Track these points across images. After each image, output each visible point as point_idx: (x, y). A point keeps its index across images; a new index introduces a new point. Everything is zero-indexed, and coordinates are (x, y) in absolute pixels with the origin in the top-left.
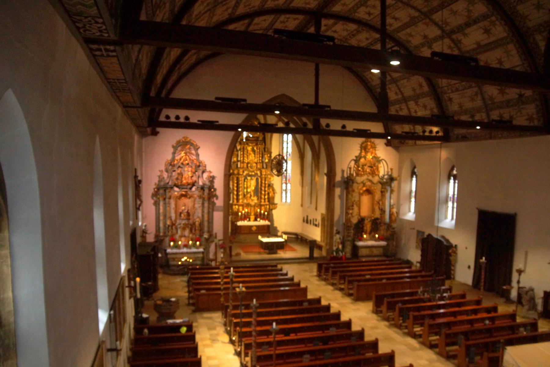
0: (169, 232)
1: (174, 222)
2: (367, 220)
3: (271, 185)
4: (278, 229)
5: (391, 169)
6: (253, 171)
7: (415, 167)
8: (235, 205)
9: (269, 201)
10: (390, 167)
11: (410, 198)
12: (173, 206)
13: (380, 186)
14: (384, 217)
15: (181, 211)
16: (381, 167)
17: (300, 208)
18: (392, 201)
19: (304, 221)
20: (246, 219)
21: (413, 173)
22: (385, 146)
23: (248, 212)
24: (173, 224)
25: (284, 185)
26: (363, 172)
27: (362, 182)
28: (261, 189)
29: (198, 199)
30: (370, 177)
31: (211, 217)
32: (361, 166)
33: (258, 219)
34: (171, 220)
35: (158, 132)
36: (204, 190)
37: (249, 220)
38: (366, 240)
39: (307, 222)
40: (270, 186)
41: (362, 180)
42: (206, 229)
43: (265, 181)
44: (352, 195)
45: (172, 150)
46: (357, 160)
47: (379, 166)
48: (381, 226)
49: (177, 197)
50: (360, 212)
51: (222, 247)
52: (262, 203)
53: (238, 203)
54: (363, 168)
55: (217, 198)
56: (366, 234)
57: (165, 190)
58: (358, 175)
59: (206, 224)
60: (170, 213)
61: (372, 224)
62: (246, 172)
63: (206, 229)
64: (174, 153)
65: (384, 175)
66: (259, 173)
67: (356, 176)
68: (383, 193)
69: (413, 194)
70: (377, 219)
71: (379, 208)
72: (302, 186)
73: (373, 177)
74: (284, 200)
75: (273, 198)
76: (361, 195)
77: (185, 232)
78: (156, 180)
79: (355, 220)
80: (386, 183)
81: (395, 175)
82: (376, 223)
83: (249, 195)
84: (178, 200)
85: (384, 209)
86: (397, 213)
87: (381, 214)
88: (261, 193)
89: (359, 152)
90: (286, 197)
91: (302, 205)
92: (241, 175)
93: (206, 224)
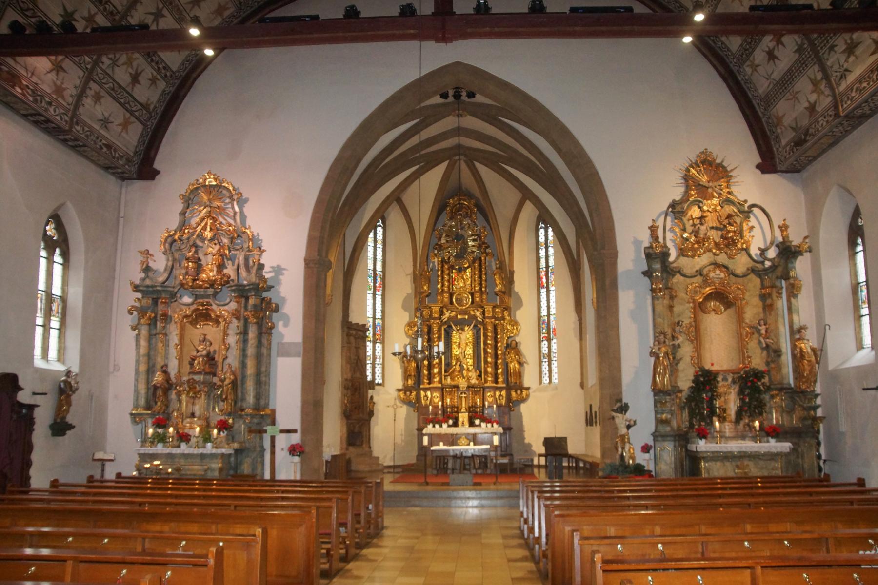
0: (156, 403)
1: (173, 380)
2: (725, 379)
3: (514, 342)
4: (534, 448)
5: (783, 228)
6: (465, 312)
7: (857, 213)
8: (426, 390)
9: (507, 381)
10: (777, 222)
11: (857, 308)
12: (174, 339)
13: (755, 281)
14: (779, 368)
15: (195, 353)
16: (752, 228)
17: (581, 391)
18: (795, 318)
19: (587, 425)
20: (446, 421)
21: (855, 232)
22: (758, 172)
23: (452, 407)
24: (168, 386)
25: (545, 344)
26: (698, 242)
27: (700, 273)
28: (486, 352)
29: (235, 322)
30: (722, 259)
31: (263, 369)
32: (689, 229)
33: (477, 422)
34: (165, 372)
35: (157, 172)
36: (247, 299)
37: (455, 424)
38: (722, 436)
39: (591, 425)
40: (513, 347)
41: (698, 268)
42: (251, 399)
43: (496, 333)
44: (671, 307)
45: (180, 207)
46: (676, 209)
47: (745, 227)
48: (772, 397)
49: (186, 317)
50: (700, 357)
51: (293, 450)
52: (488, 384)
53: (431, 385)
54: (696, 233)
55: (286, 325)
56: (722, 419)
57: (155, 302)
58: (682, 252)
59: (250, 386)
60: (166, 357)
61: (741, 392)
62: (447, 315)
63: (251, 399)
64: (183, 213)
65: (763, 251)
66: (478, 314)
67: (677, 258)
68: (769, 301)
69: (863, 294)
70: (757, 375)
71: (760, 342)
72: (581, 339)
73: (730, 257)
74: (546, 380)
75: (519, 375)
76: (701, 308)
77: (193, 404)
78: (137, 276)
79: (685, 382)
80: (774, 267)
81: (795, 240)
82: (757, 390)
83: (458, 368)
84: (189, 326)
85: (774, 346)
86: (813, 350)
87: (767, 364)
88: (486, 362)
89: (682, 189)
90: (550, 371)
91: (582, 385)
92: (435, 319)
93: (250, 386)
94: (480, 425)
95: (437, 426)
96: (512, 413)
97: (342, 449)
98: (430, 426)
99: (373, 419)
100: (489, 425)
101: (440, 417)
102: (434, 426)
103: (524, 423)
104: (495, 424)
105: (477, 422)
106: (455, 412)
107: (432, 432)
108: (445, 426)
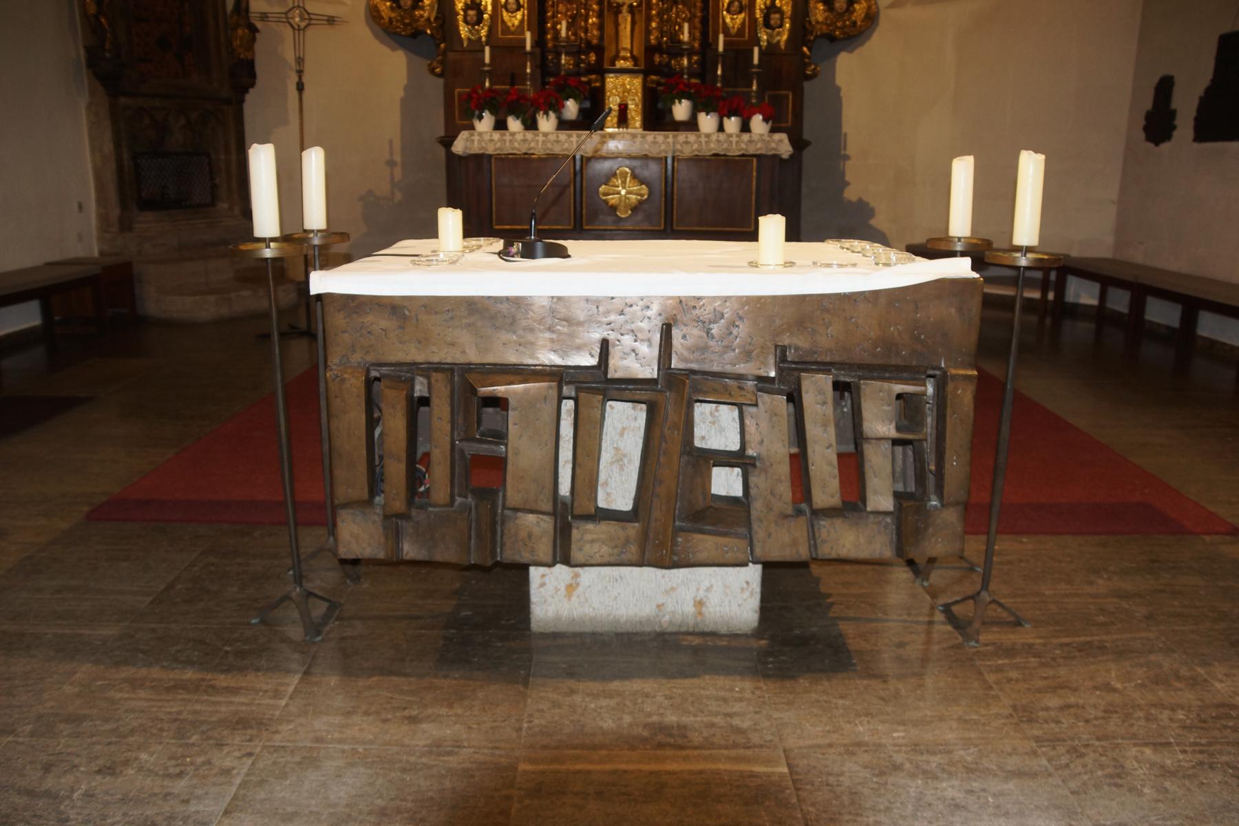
33: (681, 110)
94: (691, 125)
95: (514, 124)
96: (807, 85)
97: (103, 219)
98: (485, 124)
99: (251, 98)
100: (732, 124)
101: (529, 88)
102: (501, 125)
103: (846, 128)
104: (758, 123)
105: (681, 110)
106: (591, 70)
107: (490, 150)
108: (547, 123)
